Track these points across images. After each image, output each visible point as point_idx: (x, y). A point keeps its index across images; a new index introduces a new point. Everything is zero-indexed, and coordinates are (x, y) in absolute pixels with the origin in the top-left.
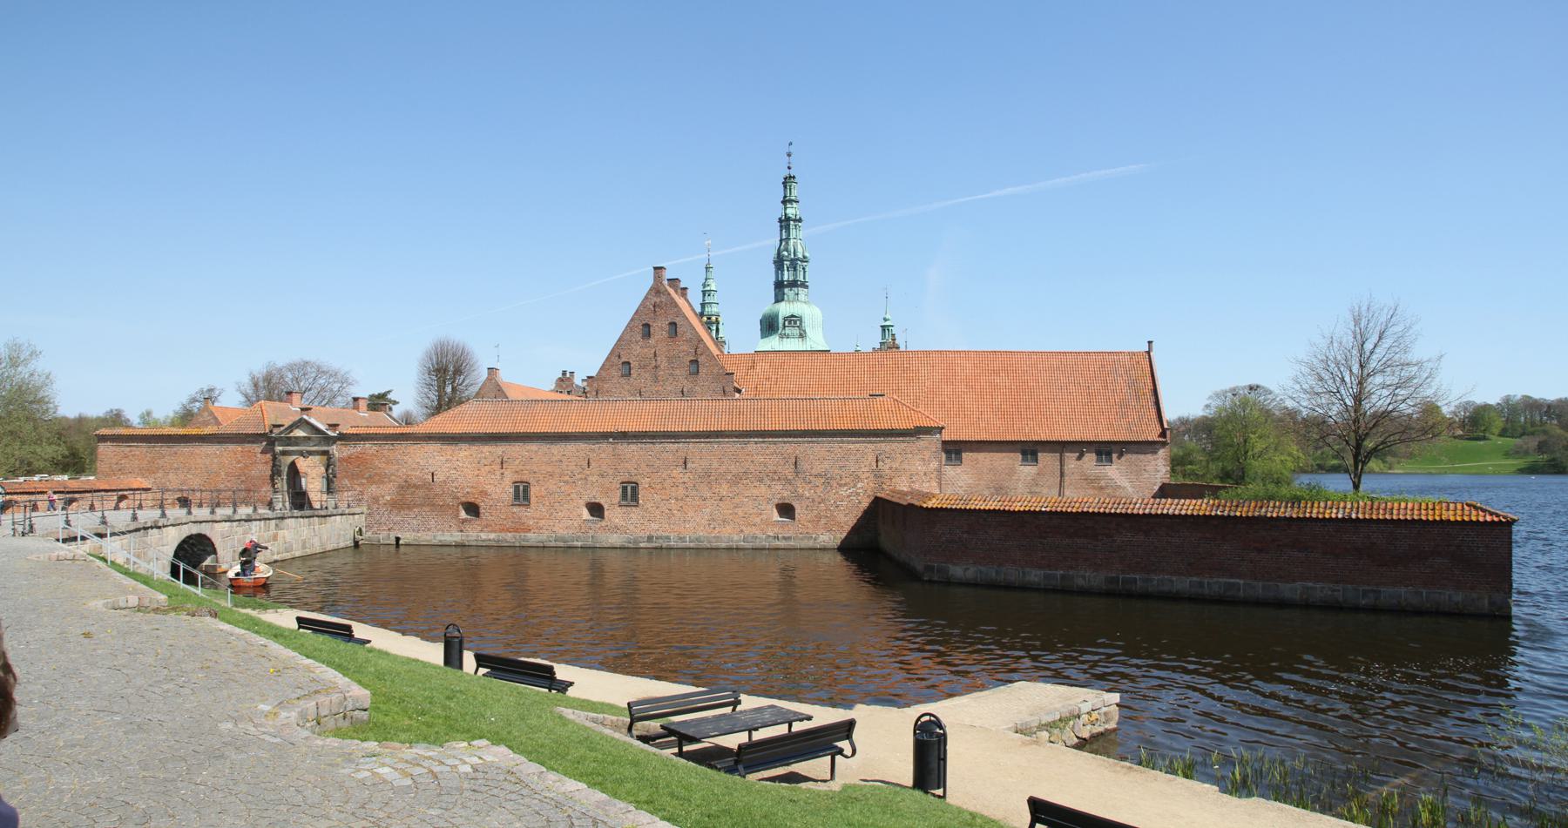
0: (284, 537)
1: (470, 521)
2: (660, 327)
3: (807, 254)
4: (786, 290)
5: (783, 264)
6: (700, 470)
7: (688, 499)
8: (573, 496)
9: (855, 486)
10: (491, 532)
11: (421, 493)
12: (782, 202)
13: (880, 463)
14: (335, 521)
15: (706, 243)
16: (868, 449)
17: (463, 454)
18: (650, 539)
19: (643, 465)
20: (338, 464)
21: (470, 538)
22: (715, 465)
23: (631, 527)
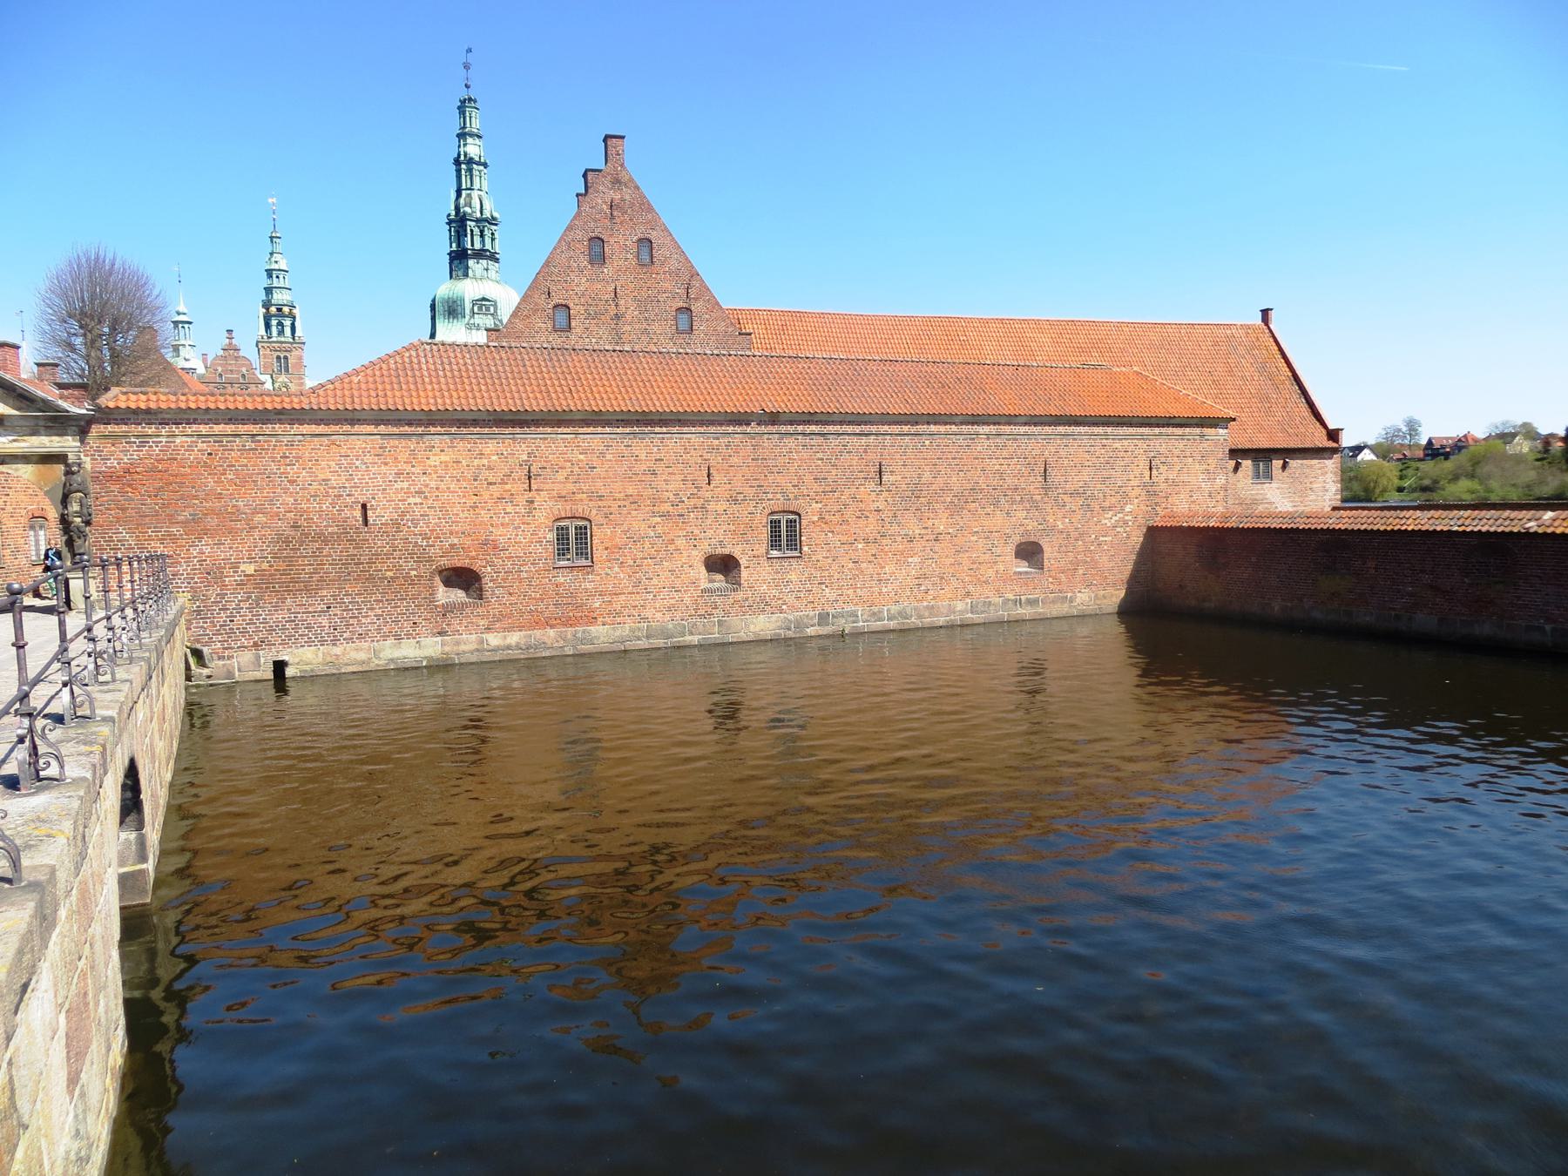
1: (463, 606)
3: (496, 215)
4: (471, 262)
5: (466, 226)
6: (904, 487)
10: (510, 629)
11: (333, 552)
12: (458, 136)
13: (1154, 472)
15: (270, 200)
16: (1132, 445)
18: (823, 618)
19: (808, 478)
20: (93, 488)
21: (463, 647)
22: (927, 476)
23: (790, 599)
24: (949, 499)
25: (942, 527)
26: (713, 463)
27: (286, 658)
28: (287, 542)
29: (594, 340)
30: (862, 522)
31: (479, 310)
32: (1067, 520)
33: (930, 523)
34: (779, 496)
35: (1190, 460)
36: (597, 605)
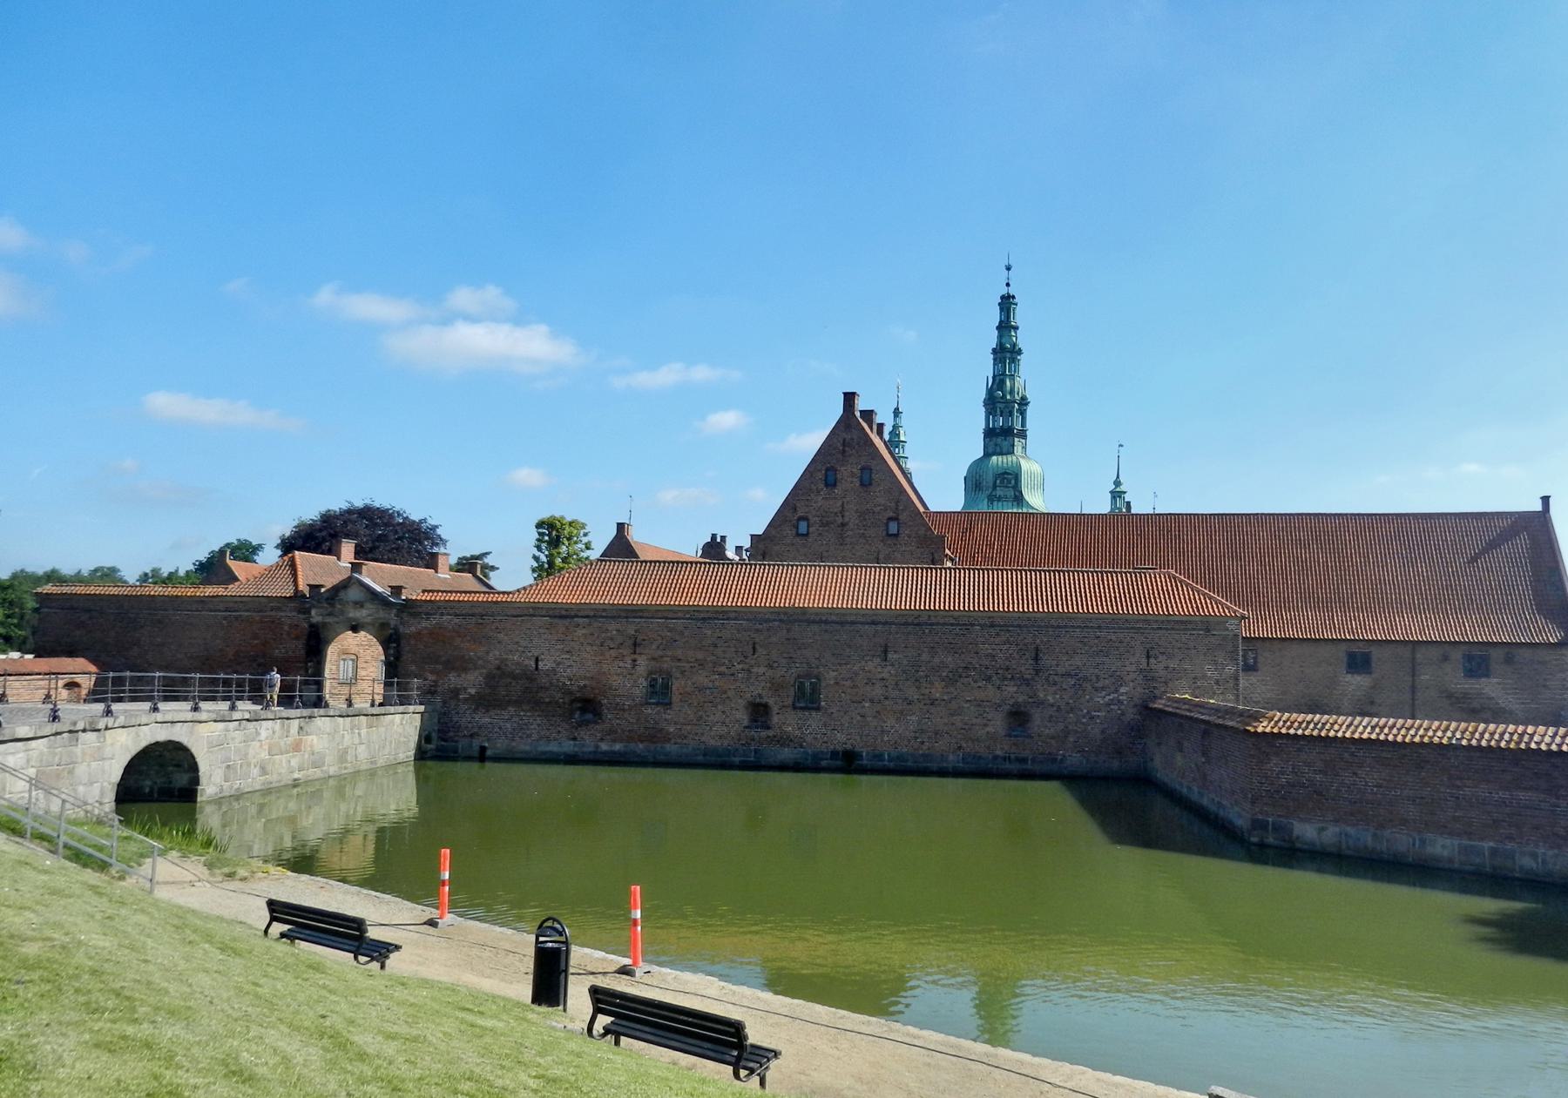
0: (311, 746)
2: (848, 472)
4: (999, 440)
7: (887, 702)
8: (730, 694)
9: (1116, 691)
10: (614, 741)
13: (1152, 661)
14: (392, 722)
17: (580, 632)
22: (925, 657)
24: (944, 674)
25: (938, 695)
26: (757, 640)
27: (487, 745)
28: (494, 677)
29: (825, 542)
30: (868, 688)
31: (1000, 483)
32: (1058, 696)
33: (927, 691)
34: (805, 665)
35: (1193, 651)
36: (672, 730)
